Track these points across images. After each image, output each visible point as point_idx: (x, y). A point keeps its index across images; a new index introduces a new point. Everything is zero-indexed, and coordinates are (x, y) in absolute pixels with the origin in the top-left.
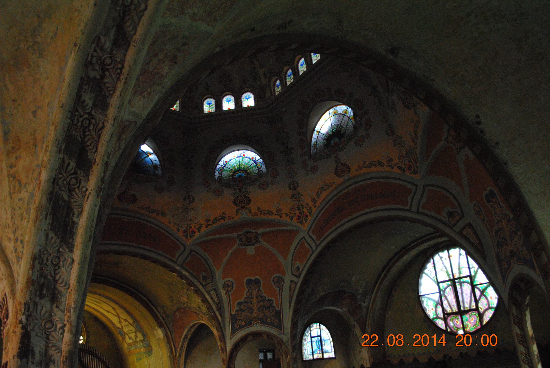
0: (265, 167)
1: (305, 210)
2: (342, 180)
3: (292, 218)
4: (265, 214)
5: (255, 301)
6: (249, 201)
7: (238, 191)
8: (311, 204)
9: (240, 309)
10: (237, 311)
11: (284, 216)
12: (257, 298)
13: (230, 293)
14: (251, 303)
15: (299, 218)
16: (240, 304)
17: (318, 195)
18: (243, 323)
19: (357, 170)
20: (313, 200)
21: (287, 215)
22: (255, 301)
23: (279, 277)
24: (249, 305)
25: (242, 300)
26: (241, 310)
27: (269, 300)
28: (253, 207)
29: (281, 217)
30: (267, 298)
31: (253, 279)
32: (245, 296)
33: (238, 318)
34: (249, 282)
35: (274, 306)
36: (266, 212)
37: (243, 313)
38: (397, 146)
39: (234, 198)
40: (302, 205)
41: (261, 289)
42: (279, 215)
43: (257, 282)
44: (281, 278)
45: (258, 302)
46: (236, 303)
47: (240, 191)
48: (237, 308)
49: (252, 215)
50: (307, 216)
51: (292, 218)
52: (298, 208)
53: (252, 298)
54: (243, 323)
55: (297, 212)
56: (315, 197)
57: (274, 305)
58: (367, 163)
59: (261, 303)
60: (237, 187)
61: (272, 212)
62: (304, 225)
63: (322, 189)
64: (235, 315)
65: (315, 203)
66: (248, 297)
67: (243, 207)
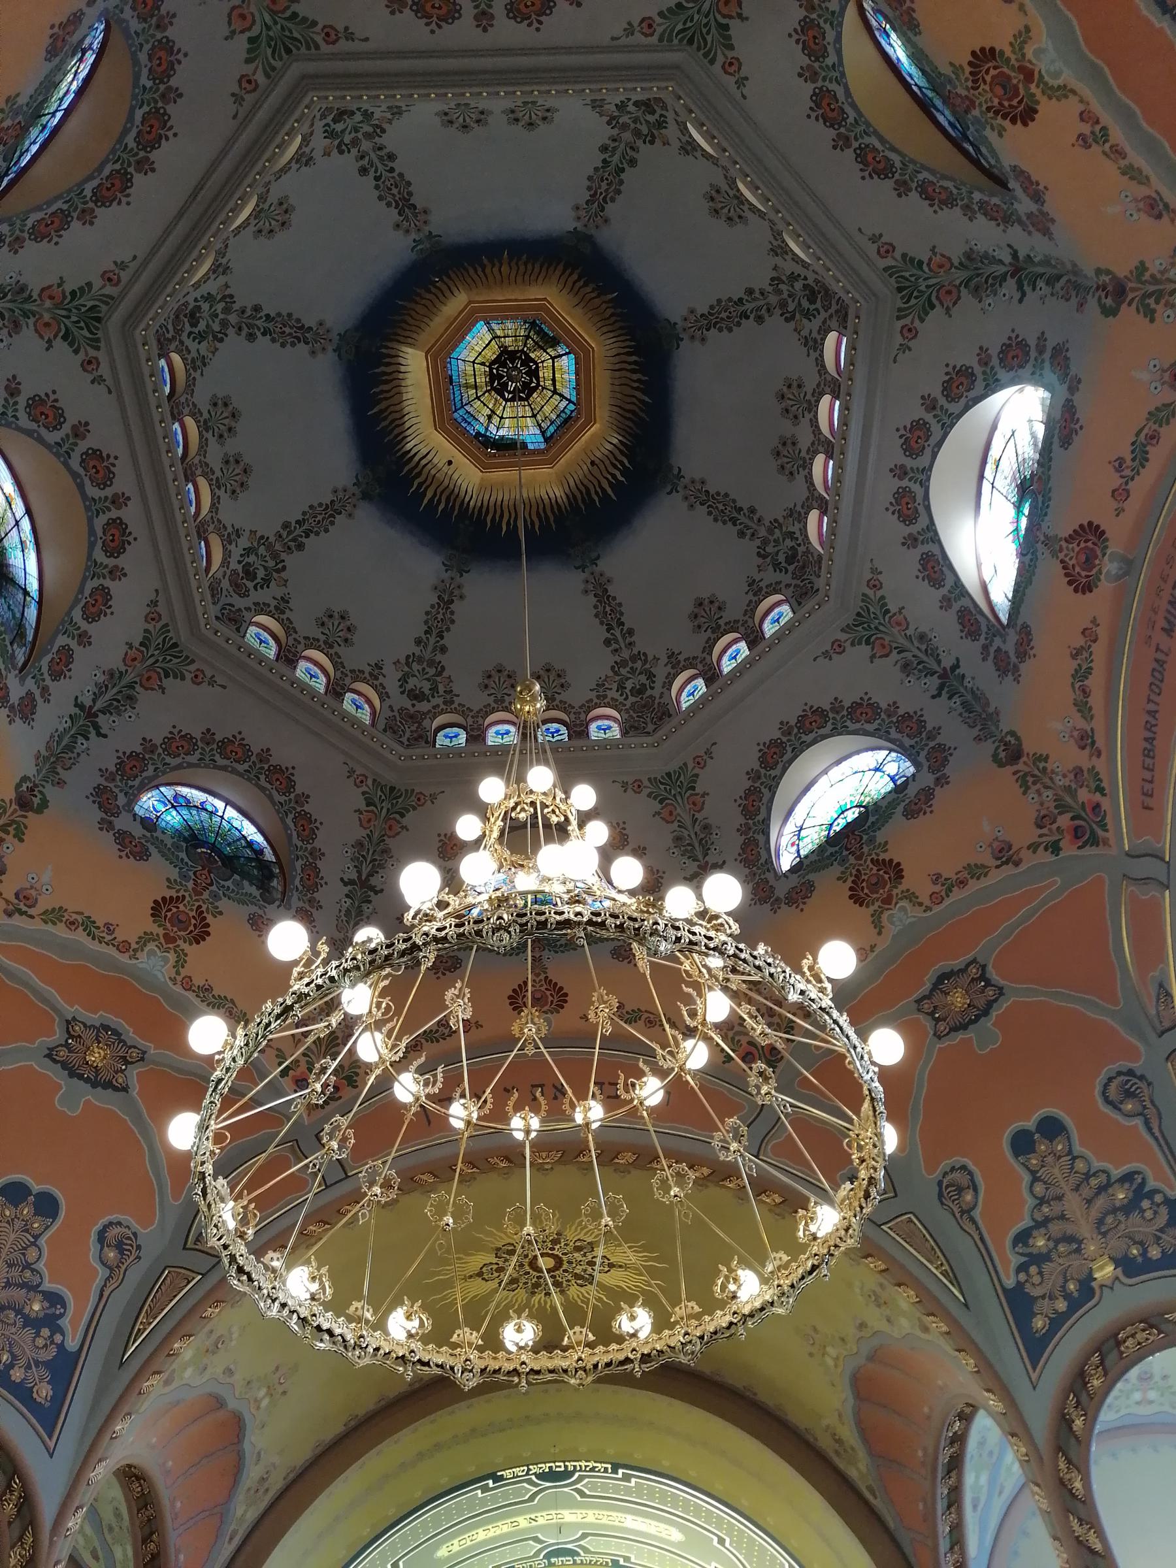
0: (908, 764)
1: (1084, 795)
2: (1105, 587)
3: (1055, 848)
4: (962, 883)
5: (1073, 1204)
6: (897, 872)
7: (852, 859)
8: (1082, 759)
9: (1029, 1255)
10: (1022, 1268)
11: (1024, 854)
12: (1077, 1189)
13: (976, 1214)
14: (1062, 1217)
15: (1077, 833)
16: (1023, 1238)
17: (1083, 707)
18: (1062, 1305)
19: (1119, 512)
20: (1085, 740)
21: (1033, 847)
22: (1073, 1204)
23: (1119, 1073)
24: (1055, 1228)
25: (1026, 1223)
26: (1039, 1259)
27: (1128, 1178)
28: (916, 880)
29: (1017, 864)
30: (1117, 1173)
31: (1030, 1124)
32: (1030, 1202)
33: (1036, 1292)
34: (1022, 1144)
35: (1156, 1191)
36: (965, 874)
37: (1047, 1267)
38: (1159, 308)
39: (849, 884)
40: (1067, 789)
41: (1078, 1149)
42: (1007, 863)
43: (1051, 1128)
44: (1130, 1073)
45: (1089, 1202)
46: (1008, 1242)
47: (859, 858)
48: (1015, 1261)
49: (928, 909)
50: (1097, 807)
51: (1055, 848)
52: (1062, 808)
53: (1059, 1198)
54: (1062, 1305)
55: (1064, 821)
56: (1082, 724)
57: (1152, 1184)
58: (1128, 457)
59: (1101, 1202)
60: (845, 853)
61: (983, 866)
62: (1106, 842)
63: (1081, 674)
64: (1020, 1285)
65: (1093, 743)
66: (1042, 1201)
67: (888, 900)
